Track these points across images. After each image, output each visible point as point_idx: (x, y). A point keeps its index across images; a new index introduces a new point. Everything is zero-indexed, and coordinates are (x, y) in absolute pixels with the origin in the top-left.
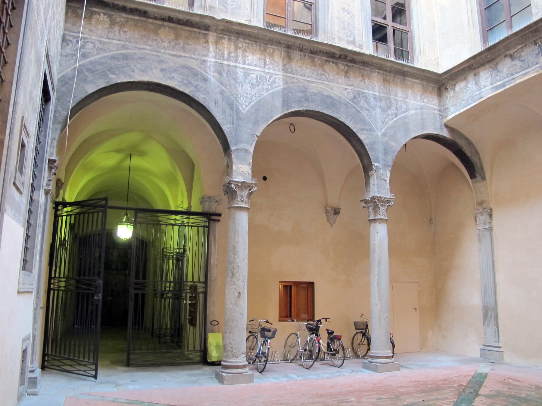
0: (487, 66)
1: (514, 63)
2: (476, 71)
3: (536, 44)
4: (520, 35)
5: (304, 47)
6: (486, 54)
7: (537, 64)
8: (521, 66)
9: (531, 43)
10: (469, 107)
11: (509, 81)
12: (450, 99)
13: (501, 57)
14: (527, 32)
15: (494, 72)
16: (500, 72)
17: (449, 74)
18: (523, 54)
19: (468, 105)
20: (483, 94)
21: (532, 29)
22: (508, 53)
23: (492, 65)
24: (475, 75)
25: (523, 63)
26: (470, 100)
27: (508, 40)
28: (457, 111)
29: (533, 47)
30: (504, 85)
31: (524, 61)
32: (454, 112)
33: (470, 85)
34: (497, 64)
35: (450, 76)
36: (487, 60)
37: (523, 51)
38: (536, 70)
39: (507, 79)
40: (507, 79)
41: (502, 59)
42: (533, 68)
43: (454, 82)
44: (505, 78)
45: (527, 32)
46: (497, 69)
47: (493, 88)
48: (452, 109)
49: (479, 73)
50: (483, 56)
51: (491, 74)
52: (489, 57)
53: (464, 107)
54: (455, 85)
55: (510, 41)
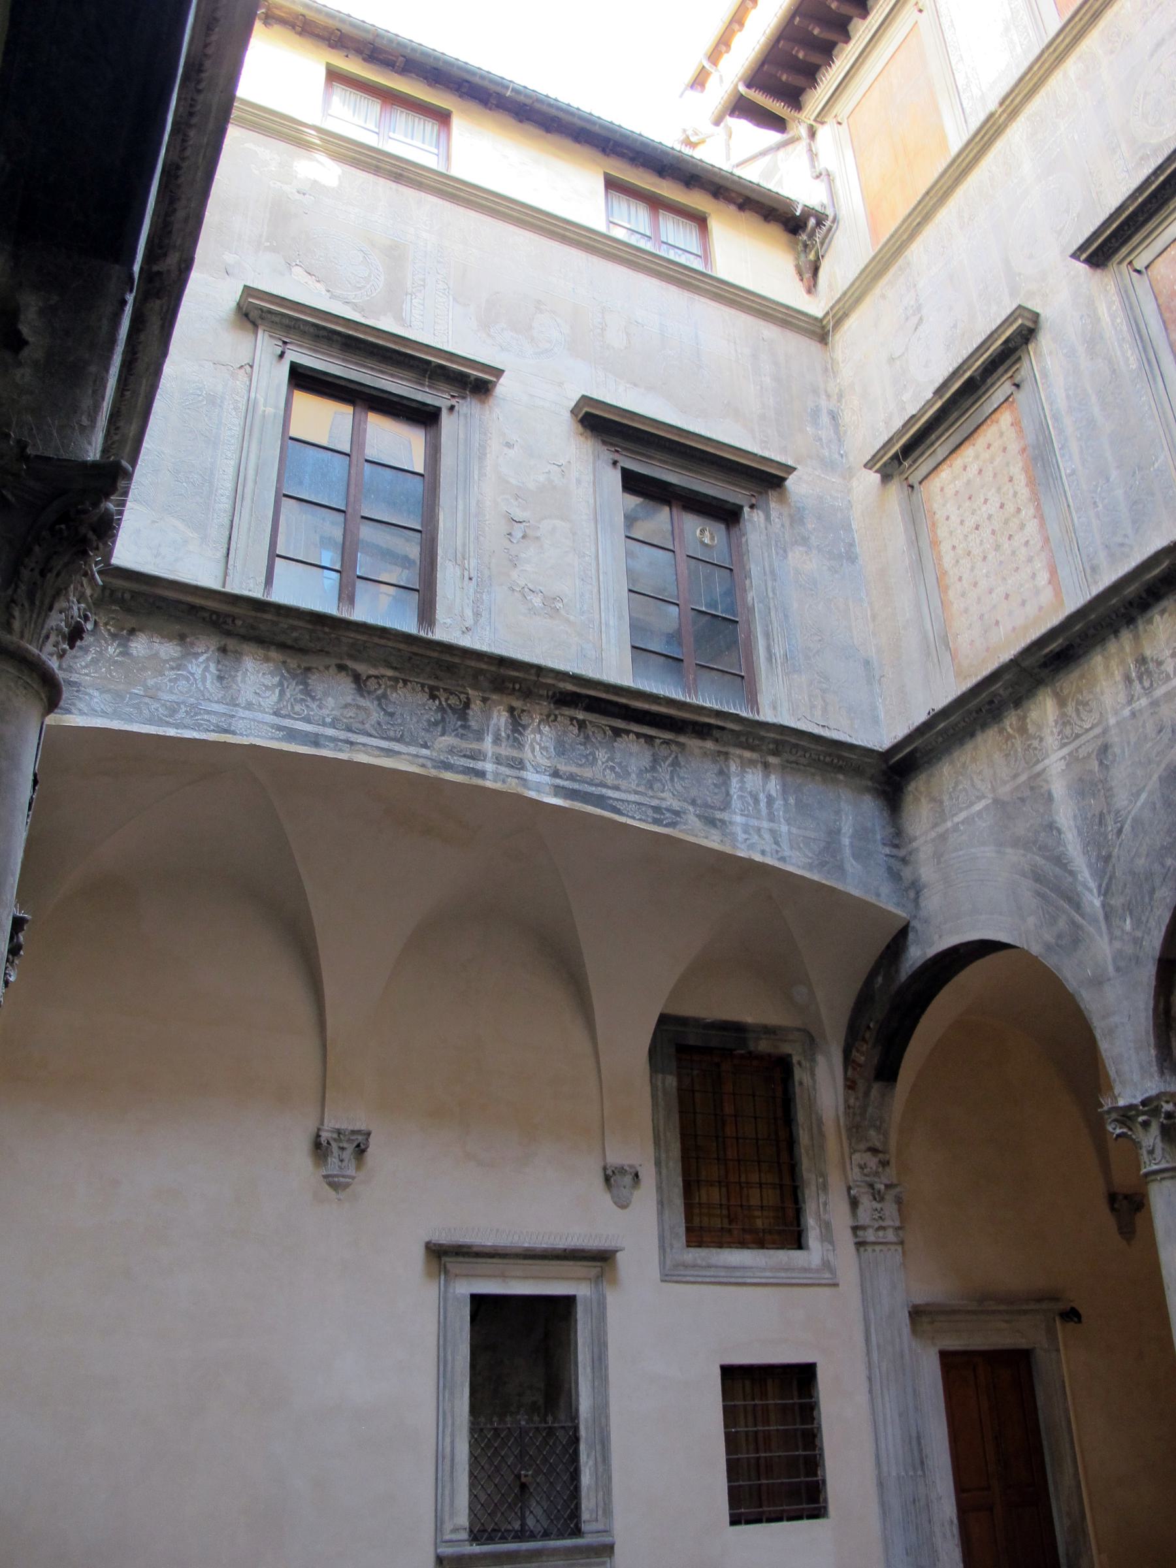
0: (273, 654)
1: (363, 702)
2: (231, 643)
3: (433, 697)
4: (415, 649)
5: (192, 133)
6: (301, 624)
7: (425, 746)
8: (379, 723)
9: (423, 686)
10: (172, 732)
11: (334, 740)
12: (94, 661)
13: (328, 661)
14: (435, 655)
15: (293, 689)
16: (313, 698)
17: (144, 588)
18: (393, 696)
19: (168, 724)
20: (239, 725)
21: (448, 658)
22: (350, 664)
23: (293, 664)
24: (223, 650)
25: (387, 718)
26: (181, 714)
27: (381, 637)
28: (116, 715)
29: (422, 698)
30: (315, 740)
31: (392, 715)
32: (104, 714)
33: (196, 667)
34: (308, 669)
35: (135, 595)
36: (281, 638)
37: (394, 688)
38: (421, 761)
39: (330, 732)
40: (330, 732)
41: (327, 668)
42: (413, 750)
43: (132, 622)
44: (324, 724)
45: (435, 655)
46: (306, 684)
47: (280, 728)
48: (98, 699)
49: (238, 656)
50: (285, 623)
51: (280, 684)
52: (295, 634)
53: (150, 721)
54: (132, 632)
55: (383, 642)
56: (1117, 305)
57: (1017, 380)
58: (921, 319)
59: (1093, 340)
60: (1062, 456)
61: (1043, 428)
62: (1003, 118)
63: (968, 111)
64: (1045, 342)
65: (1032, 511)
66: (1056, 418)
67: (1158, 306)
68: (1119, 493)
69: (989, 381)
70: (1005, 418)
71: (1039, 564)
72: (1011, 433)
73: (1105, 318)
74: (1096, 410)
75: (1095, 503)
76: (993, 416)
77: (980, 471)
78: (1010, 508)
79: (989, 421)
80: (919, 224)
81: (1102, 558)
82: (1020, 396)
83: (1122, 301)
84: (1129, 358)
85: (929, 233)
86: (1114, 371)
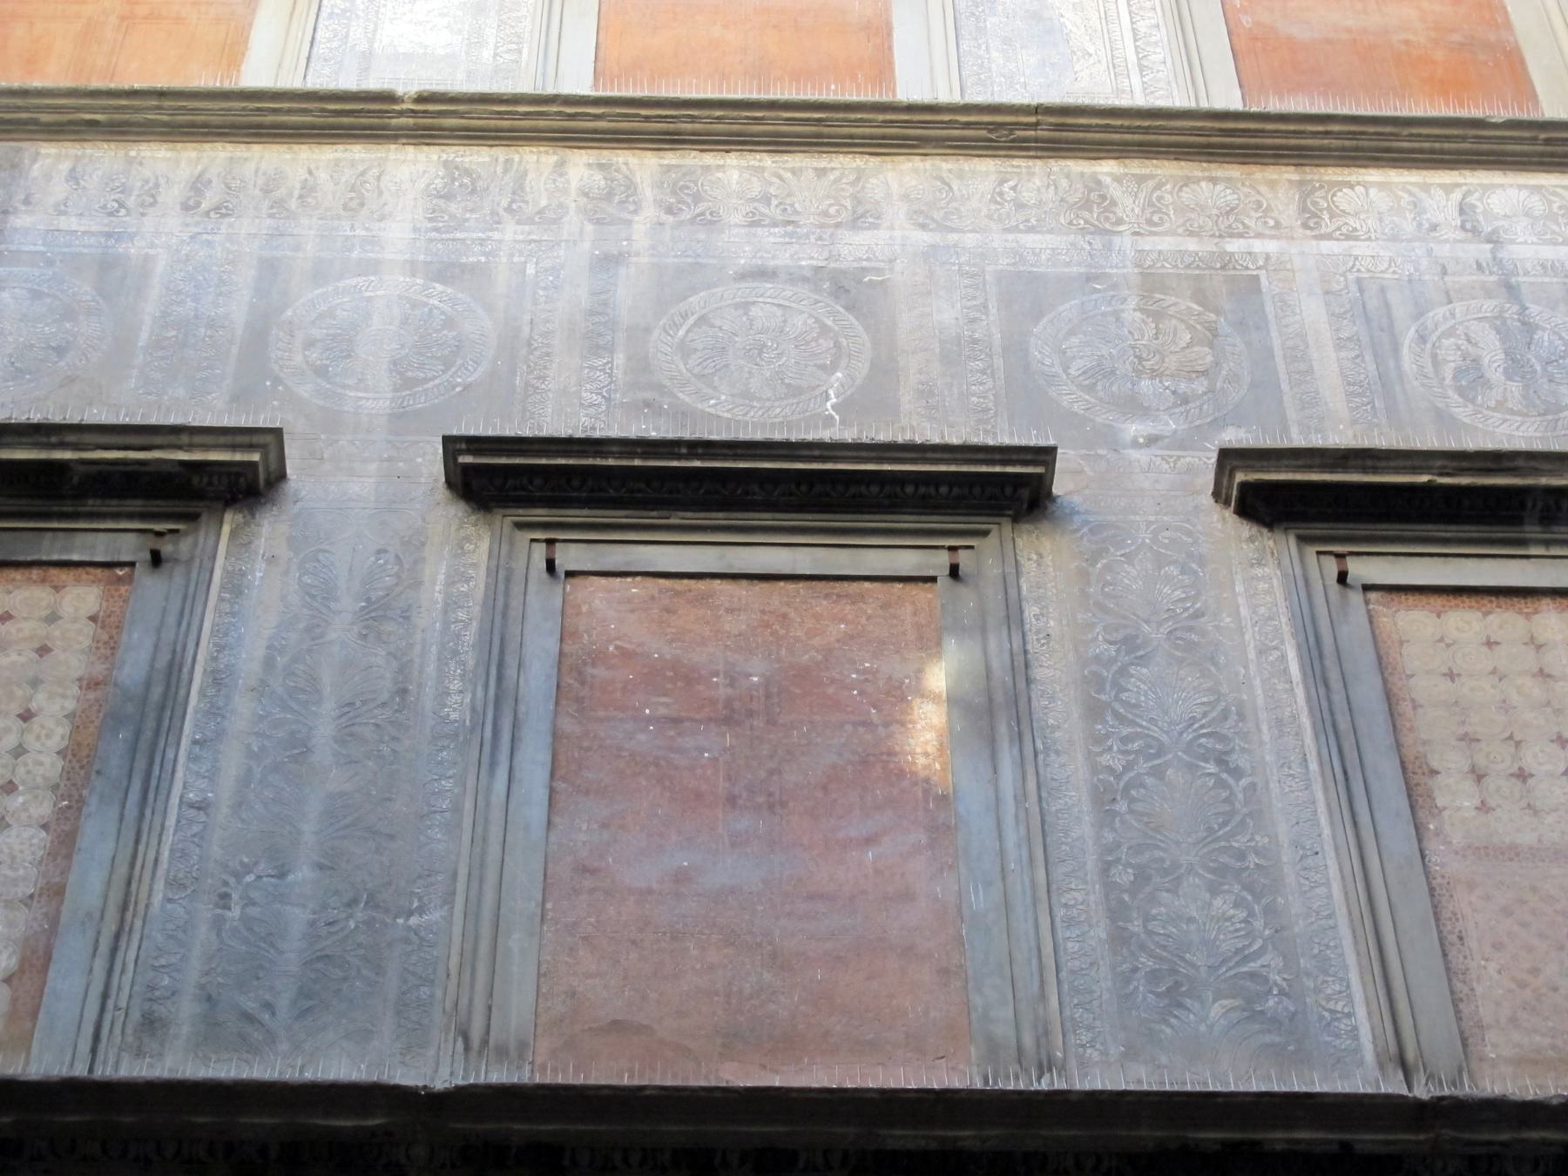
57: (167, 548)
59: (382, 612)
60: (193, 758)
62: (403, 121)
63: (319, 50)
64: (270, 530)
65: (44, 808)
66: (217, 679)
67: (561, 653)
68: (298, 917)
69: (92, 504)
70: (82, 598)
74: (324, 731)
75: (225, 896)
76: (54, 572)
79: (35, 573)
80: (93, 124)
81: (186, 1010)
82: (151, 588)
84: (454, 697)
85: (103, 158)
86: (403, 692)
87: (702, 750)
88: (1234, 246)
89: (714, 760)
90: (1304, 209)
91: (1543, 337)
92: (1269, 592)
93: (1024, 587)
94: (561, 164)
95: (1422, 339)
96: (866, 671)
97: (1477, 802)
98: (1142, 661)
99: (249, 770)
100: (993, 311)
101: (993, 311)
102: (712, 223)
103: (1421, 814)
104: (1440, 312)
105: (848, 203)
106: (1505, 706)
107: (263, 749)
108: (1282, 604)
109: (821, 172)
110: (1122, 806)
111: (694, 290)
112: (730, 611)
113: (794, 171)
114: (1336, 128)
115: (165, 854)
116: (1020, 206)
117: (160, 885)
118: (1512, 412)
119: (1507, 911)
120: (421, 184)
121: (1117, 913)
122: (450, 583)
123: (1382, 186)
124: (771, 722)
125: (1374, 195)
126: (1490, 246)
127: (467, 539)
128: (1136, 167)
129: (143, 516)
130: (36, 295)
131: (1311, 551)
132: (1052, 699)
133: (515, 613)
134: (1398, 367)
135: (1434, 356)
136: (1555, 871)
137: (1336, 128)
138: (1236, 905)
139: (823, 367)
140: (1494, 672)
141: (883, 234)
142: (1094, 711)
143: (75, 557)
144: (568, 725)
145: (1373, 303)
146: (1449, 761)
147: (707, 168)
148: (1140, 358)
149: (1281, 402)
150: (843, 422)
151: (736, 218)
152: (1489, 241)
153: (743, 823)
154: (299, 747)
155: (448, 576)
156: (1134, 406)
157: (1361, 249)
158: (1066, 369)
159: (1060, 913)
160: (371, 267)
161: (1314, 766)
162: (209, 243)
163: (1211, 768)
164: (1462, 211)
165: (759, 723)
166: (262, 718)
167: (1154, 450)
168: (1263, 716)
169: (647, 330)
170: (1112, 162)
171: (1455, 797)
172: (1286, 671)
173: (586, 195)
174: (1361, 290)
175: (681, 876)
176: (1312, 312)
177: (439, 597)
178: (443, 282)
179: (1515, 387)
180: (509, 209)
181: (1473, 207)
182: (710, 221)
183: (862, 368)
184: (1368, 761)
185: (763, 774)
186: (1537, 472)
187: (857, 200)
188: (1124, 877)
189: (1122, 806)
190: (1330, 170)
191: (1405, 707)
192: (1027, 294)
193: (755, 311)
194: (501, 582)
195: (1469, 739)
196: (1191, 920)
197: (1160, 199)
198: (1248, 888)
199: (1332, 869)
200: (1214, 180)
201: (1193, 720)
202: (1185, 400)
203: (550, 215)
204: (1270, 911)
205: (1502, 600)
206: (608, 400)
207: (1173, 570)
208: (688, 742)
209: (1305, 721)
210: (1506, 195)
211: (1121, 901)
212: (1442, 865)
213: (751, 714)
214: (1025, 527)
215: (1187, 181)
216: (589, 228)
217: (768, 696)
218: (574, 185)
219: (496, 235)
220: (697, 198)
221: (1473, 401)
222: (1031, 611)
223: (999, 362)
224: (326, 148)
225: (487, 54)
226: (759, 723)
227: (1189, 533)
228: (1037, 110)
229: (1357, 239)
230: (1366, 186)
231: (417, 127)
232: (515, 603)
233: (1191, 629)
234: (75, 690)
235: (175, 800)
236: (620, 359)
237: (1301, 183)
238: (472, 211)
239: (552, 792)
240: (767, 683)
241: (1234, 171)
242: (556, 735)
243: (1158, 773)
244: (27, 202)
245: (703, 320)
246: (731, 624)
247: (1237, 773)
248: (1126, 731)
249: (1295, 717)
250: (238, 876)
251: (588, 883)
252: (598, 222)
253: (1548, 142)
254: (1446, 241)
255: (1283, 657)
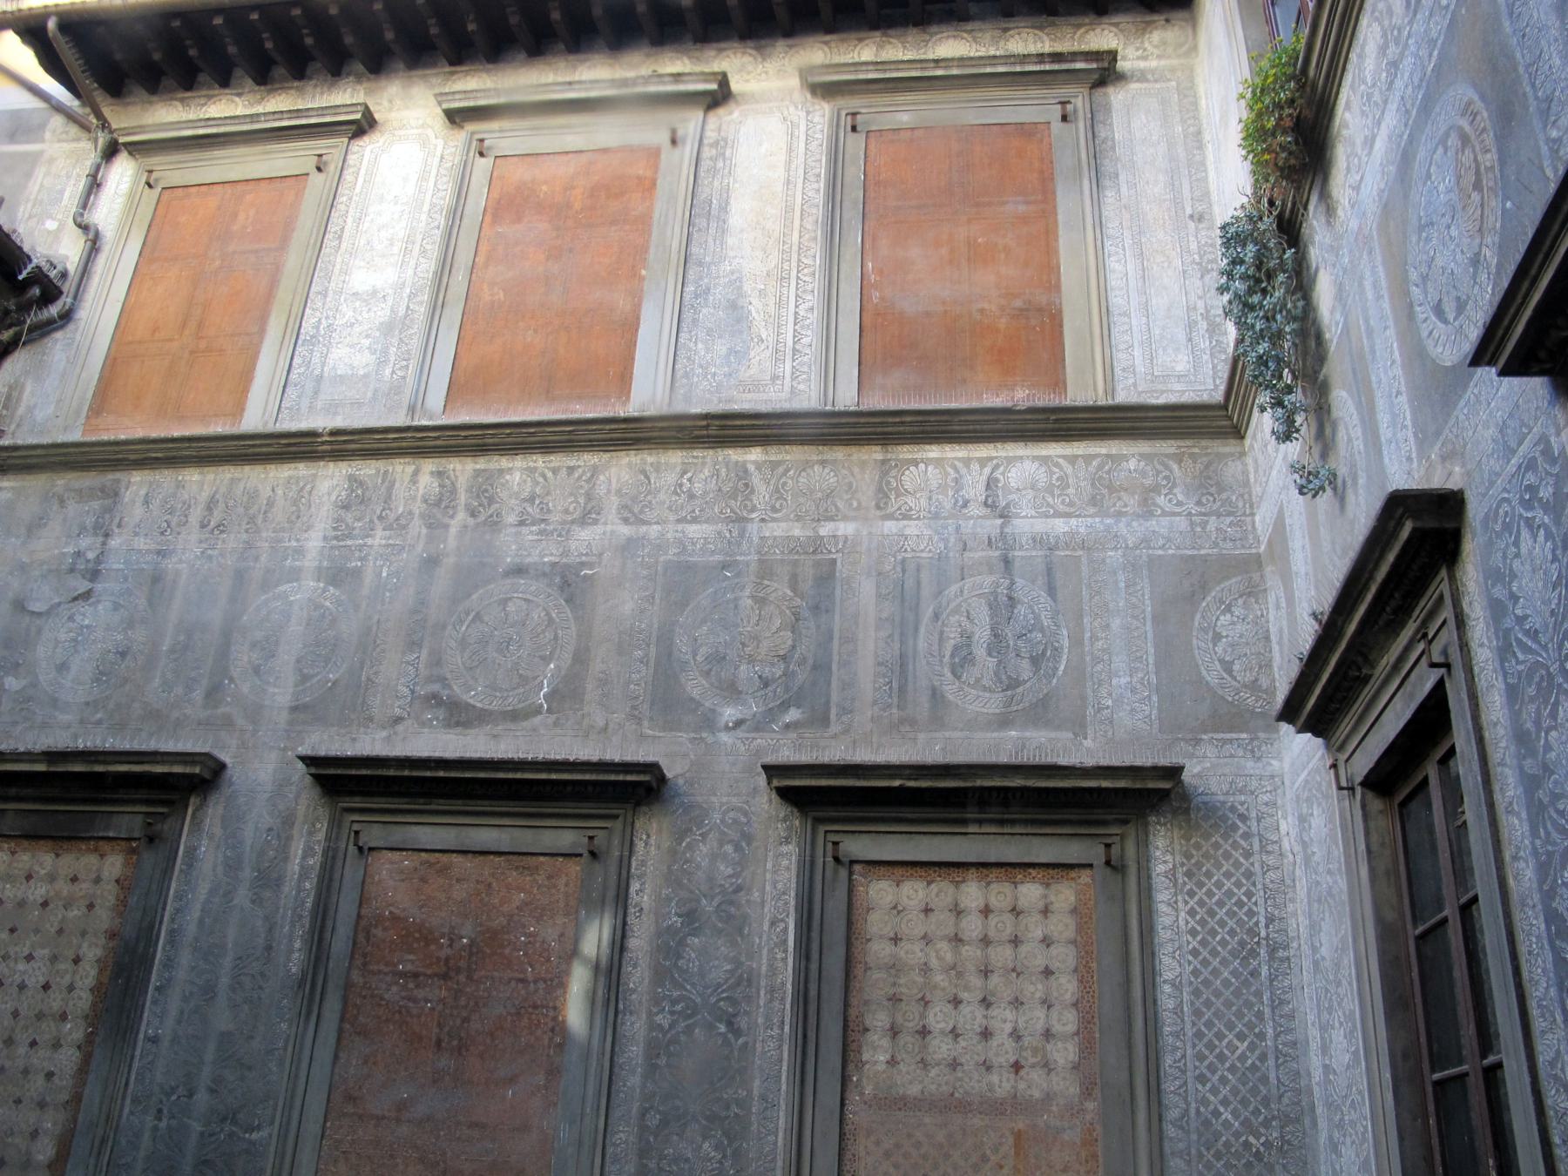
56: (315, 861)
58: (87, 595)
59: (268, 879)
60: (155, 1002)
61: (148, 933)
64: (214, 812)
67: (359, 916)
70: (114, 865)
71: (51, 1123)
72: (108, 894)
73: (294, 866)
75: (160, 1111)
77: (45, 904)
78: (55, 1002)
82: (149, 858)
83: (323, 866)
86: (269, 948)
87: (427, 1001)
88: (825, 530)
89: (432, 1009)
90: (880, 490)
91: (1021, 610)
92: (788, 869)
93: (634, 864)
94: (416, 473)
95: (936, 616)
96: (531, 935)
97: (888, 1057)
98: (695, 932)
99: (182, 1012)
100: (657, 601)
101: (657, 601)
102: (496, 523)
103: (851, 1067)
104: (954, 588)
105: (582, 500)
106: (926, 969)
107: (191, 993)
108: (794, 885)
109: (571, 469)
110: (662, 1061)
111: (476, 587)
112: (458, 880)
113: (555, 471)
114: (908, 419)
115: (133, 1077)
116: (692, 496)
117: (128, 1101)
118: (985, 689)
119: (887, 1154)
120: (333, 498)
121: (643, 1153)
122: (304, 858)
123: (938, 462)
124: (469, 978)
125: (933, 469)
126: (999, 521)
127: (317, 819)
128: (776, 454)
129: (148, 802)
130: (116, 607)
131: (822, 829)
132: (635, 966)
133: (336, 884)
134: (915, 645)
135: (942, 633)
136: (927, 1120)
137: (908, 419)
138: (716, 1148)
139: (543, 658)
140: (924, 937)
141: (599, 529)
142: (660, 975)
143: (111, 834)
144: (356, 976)
145: (910, 583)
146: (879, 1020)
147: (501, 471)
148: (743, 644)
149: (829, 684)
150: (549, 711)
151: (512, 519)
152: (1001, 517)
153: (444, 1062)
154: (209, 992)
155: (304, 851)
156: (732, 691)
157: (912, 528)
158: (695, 655)
159: (610, 1150)
160: (295, 575)
161: (787, 1029)
162: (210, 557)
163: (722, 1028)
164: (988, 486)
165: (462, 978)
166: (193, 968)
167: (740, 733)
168: (763, 983)
169: (444, 627)
170: (759, 449)
171: (876, 1053)
172: (785, 941)
173: (426, 501)
174: (904, 571)
175: (401, 1106)
176: (867, 589)
177: (297, 868)
178: (336, 586)
179: (992, 662)
180: (380, 518)
181: (997, 480)
182: (494, 524)
183: (567, 657)
184: (823, 1024)
185: (458, 1022)
186: (976, 776)
187: (589, 497)
188: (653, 1120)
189: (662, 1061)
190: (906, 448)
191: (858, 970)
192: (682, 580)
193: (511, 607)
194: (331, 860)
195: (895, 999)
196: (687, 1160)
197: (785, 484)
198: (726, 1134)
199: (783, 1119)
200: (823, 463)
201: (719, 985)
202: (766, 683)
203: (403, 522)
204: (737, 1154)
205: (944, 870)
206: (413, 692)
207: (729, 848)
208: (420, 994)
209: (789, 986)
210: (1024, 466)
211: (648, 1142)
212: (854, 1114)
213: (458, 970)
214: (644, 809)
215: (806, 465)
216: (424, 531)
217: (471, 954)
218: (421, 492)
219: (369, 541)
220: (491, 500)
221: (959, 678)
222: (635, 886)
223: (653, 649)
224: (286, 466)
225: (388, 371)
226: (462, 978)
227: (746, 814)
228: (707, 416)
229: (909, 518)
230: (927, 462)
231: (333, 451)
232: (337, 876)
233: (731, 903)
234: (102, 941)
235: (141, 1036)
236: (425, 653)
237: (884, 462)
238: (359, 520)
239: (340, 1031)
240: (472, 942)
241: (839, 453)
242: (348, 986)
243: (689, 1030)
244: (119, 526)
245: (478, 617)
246: (459, 892)
247: (737, 1033)
248: (676, 994)
249: (783, 984)
250: (168, 1095)
251: (350, 1109)
252: (429, 526)
253: (1056, 421)
254: (971, 518)
255: (786, 929)
